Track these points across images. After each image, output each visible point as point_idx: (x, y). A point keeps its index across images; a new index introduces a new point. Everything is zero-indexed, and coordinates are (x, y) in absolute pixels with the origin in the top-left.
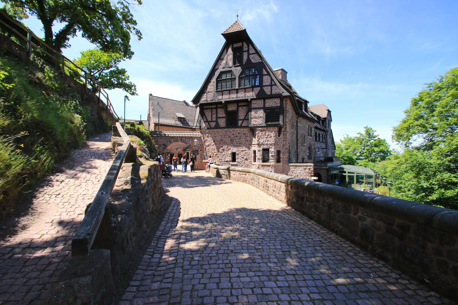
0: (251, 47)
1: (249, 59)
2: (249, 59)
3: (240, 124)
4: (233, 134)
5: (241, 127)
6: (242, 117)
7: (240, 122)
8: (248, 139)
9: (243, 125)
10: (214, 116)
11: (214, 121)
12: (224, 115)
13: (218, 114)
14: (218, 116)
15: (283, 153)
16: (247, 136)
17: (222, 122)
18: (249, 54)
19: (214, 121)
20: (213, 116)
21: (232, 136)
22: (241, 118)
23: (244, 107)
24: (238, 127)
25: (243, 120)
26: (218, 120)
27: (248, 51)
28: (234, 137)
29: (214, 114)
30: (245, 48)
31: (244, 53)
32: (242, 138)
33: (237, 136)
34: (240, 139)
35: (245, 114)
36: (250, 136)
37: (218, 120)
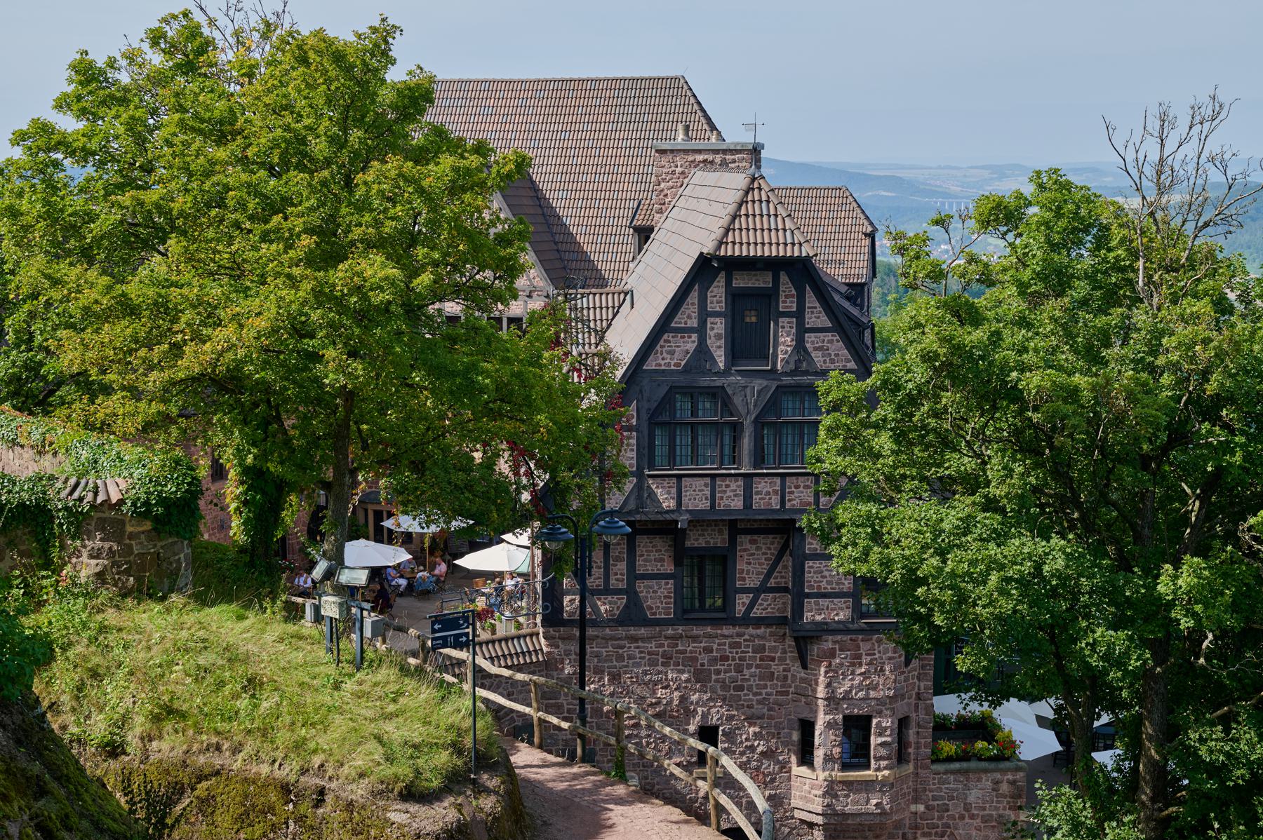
0: (811, 300)
3: (740, 609)
4: (708, 650)
5: (747, 621)
6: (752, 581)
7: (742, 601)
8: (777, 668)
9: (757, 612)
10: (622, 567)
11: (618, 592)
12: (669, 568)
14: (640, 571)
15: (919, 726)
16: (773, 659)
17: (658, 598)
18: (802, 331)
19: (618, 592)
20: (613, 569)
21: (704, 658)
22: (749, 583)
23: (760, 539)
25: (757, 592)
26: (641, 586)
27: (799, 315)
28: (714, 661)
29: (618, 559)
30: (787, 302)
34: (739, 670)
35: (765, 568)
36: (782, 659)
37: (641, 586)
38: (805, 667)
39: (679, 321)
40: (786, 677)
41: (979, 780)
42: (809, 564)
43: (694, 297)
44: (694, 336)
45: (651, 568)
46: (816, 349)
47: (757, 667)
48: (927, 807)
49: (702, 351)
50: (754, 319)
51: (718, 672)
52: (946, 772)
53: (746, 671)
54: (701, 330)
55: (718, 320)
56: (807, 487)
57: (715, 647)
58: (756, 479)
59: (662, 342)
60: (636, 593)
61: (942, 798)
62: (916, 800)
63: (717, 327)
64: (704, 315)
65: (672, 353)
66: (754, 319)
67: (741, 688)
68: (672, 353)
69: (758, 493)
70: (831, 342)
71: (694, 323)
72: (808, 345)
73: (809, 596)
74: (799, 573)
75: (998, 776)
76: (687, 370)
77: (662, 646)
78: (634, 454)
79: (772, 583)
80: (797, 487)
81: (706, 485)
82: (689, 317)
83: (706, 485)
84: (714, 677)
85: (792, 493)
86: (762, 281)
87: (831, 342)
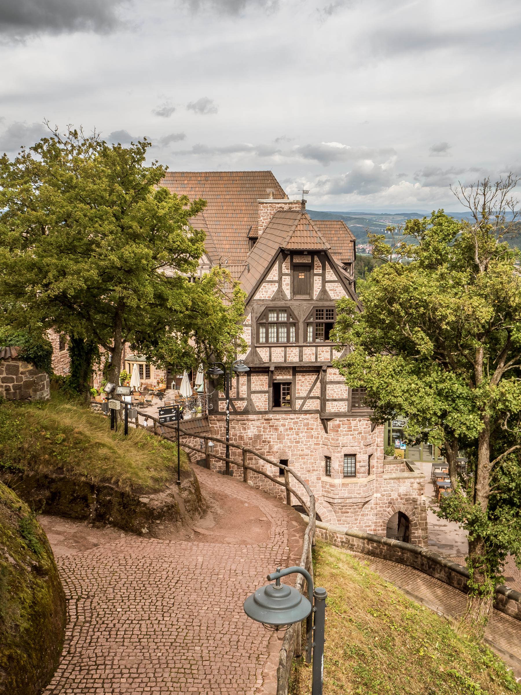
1: (324, 291)
2: (324, 291)
4: (284, 425)
5: (301, 412)
6: (304, 394)
7: (298, 403)
9: (305, 408)
13: (253, 385)
14: (253, 389)
15: (378, 459)
16: (312, 429)
18: (324, 282)
24: (295, 412)
25: (305, 399)
26: (253, 397)
27: (323, 275)
29: (242, 385)
31: (316, 278)
32: (302, 432)
33: (291, 429)
37: (253, 397)
38: (326, 432)
39: (269, 277)
40: (318, 437)
41: (404, 482)
42: (328, 386)
43: (276, 266)
44: (277, 284)
45: (258, 389)
46: (331, 290)
47: (306, 432)
48: (383, 495)
49: (280, 290)
50: (303, 277)
51: (288, 435)
52: (390, 479)
53: (300, 435)
54: (280, 281)
55: (287, 277)
56: (327, 352)
57: (287, 424)
58: (304, 348)
59: (262, 287)
60: (251, 400)
61: (388, 491)
62: (377, 492)
63: (287, 280)
64: (281, 275)
65: (267, 292)
66: (303, 277)
67: (298, 442)
68: (267, 292)
69: (305, 354)
70: (337, 287)
71: (276, 278)
72: (327, 288)
73: (328, 400)
74: (323, 390)
75: (412, 480)
76: (274, 299)
77: (263, 423)
78: (250, 337)
79: (312, 395)
80: (323, 352)
81: (282, 351)
82: (274, 276)
83: (282, 351)
84: (286, 437)
85: (320, 354)
86: (307, 260)
87: (337, 287)
